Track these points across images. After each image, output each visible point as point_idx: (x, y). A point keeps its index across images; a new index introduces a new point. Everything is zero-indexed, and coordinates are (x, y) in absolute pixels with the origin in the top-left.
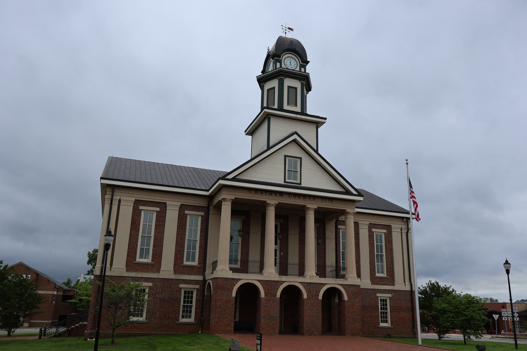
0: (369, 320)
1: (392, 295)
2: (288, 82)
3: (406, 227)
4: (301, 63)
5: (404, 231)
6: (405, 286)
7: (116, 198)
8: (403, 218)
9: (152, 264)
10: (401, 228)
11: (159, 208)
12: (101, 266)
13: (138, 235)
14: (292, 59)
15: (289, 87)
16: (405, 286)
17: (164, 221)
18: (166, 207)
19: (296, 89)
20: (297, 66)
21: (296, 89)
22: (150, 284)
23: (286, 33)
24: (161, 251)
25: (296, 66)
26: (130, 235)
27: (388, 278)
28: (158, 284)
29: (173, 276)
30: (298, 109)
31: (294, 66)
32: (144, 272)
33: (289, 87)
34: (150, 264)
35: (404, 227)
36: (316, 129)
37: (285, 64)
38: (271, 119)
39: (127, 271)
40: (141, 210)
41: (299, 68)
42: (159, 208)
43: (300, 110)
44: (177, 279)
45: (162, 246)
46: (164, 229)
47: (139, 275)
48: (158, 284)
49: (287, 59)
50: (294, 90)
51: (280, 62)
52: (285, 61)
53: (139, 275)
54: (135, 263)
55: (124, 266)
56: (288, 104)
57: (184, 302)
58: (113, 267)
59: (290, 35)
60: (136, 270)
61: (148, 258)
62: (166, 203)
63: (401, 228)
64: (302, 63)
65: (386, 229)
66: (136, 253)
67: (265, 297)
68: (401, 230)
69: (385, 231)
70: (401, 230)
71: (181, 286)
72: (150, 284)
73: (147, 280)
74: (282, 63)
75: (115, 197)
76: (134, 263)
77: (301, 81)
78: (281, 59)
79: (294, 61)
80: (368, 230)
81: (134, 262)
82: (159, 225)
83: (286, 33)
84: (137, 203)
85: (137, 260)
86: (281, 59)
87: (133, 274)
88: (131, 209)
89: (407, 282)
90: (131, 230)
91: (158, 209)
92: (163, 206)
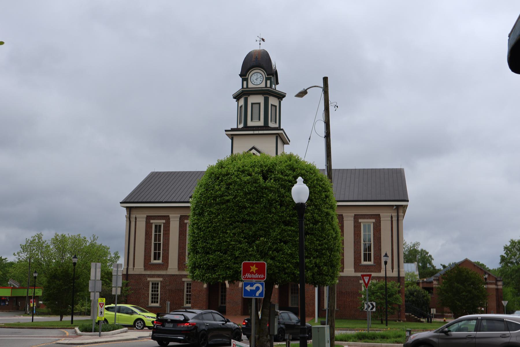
0: (351, 304)
1: (377, 281)
2: (252, 99)
3: (396, 214)
4: (266, 76)
5: (395, 219)
6: (393, 272)
7: (133, 216)
8: (393, 206)
9: (162, 264)
10: (392, 216)
11: (165, 221)
12: (126, 267)
13: (151, 243)
14: (258, 74)
15: (252, 104)
16: (393, 272)
17: (169, 230)
18: (169, 219)
19: (259, 104)
20: (263, 80)
21: (259, 104)
22: (161, 279)
23: (260, 44)
24: (168, 253)
25: (262, 80)
26: (146, 243)
27: (375, 266)
28: (167, 279)
29: (177, 272)
30: (261, 123)
31: (261, 81)
32: (157, 270)
33: (252, 104)
34: (161, 264)
35: (395, 214)
36: (275, 139)
37: (252, 80)
38: (234, 139)
39: (145, 270)
40: (152, 223)
41: (265, 82)
42: (165, 221)
43: (263, 124)
44: (181, 275)
45: (168, 250)
46: (169, 237)
47: (153, 272)
48: (167, 279)
49: (253, 76)
50: (258, 105)
51: (247, 80)
52: (252, 78)
53: (153, 272)
54: (150, 264)
55: (142, 267)
56: (252, 120)
57: (187, 292)
58: (135, 268)
59: (264, 47)
60: (151, 269)
61: (160, 259)
62: (169, 216)
63: (392, 216)
64: (267, 75)
65: (374, 219)
66: (150, 256)
67: (229, 287)
68: (392, 217)
69: (374, 220)
70: (392, 217)
71: (184, 280)
72: (161, 279)
73: (159, 276)
74: (249, 81)
75: (132, 216)
76: (149, 264)
77: (264, 96)
78: (247, 77)
79: (260, 75)
80: (353, 222)
81: (150, 263)
82: (166, 234)
83: (260, 44)
84: (148, 218)
85: (152, 262)
86: (247, 77)
87: (148, 272)
88: (144, 223)
89: (396, 269)
90: (146, 239)
91: (164, 221)
92: (167, 218)
